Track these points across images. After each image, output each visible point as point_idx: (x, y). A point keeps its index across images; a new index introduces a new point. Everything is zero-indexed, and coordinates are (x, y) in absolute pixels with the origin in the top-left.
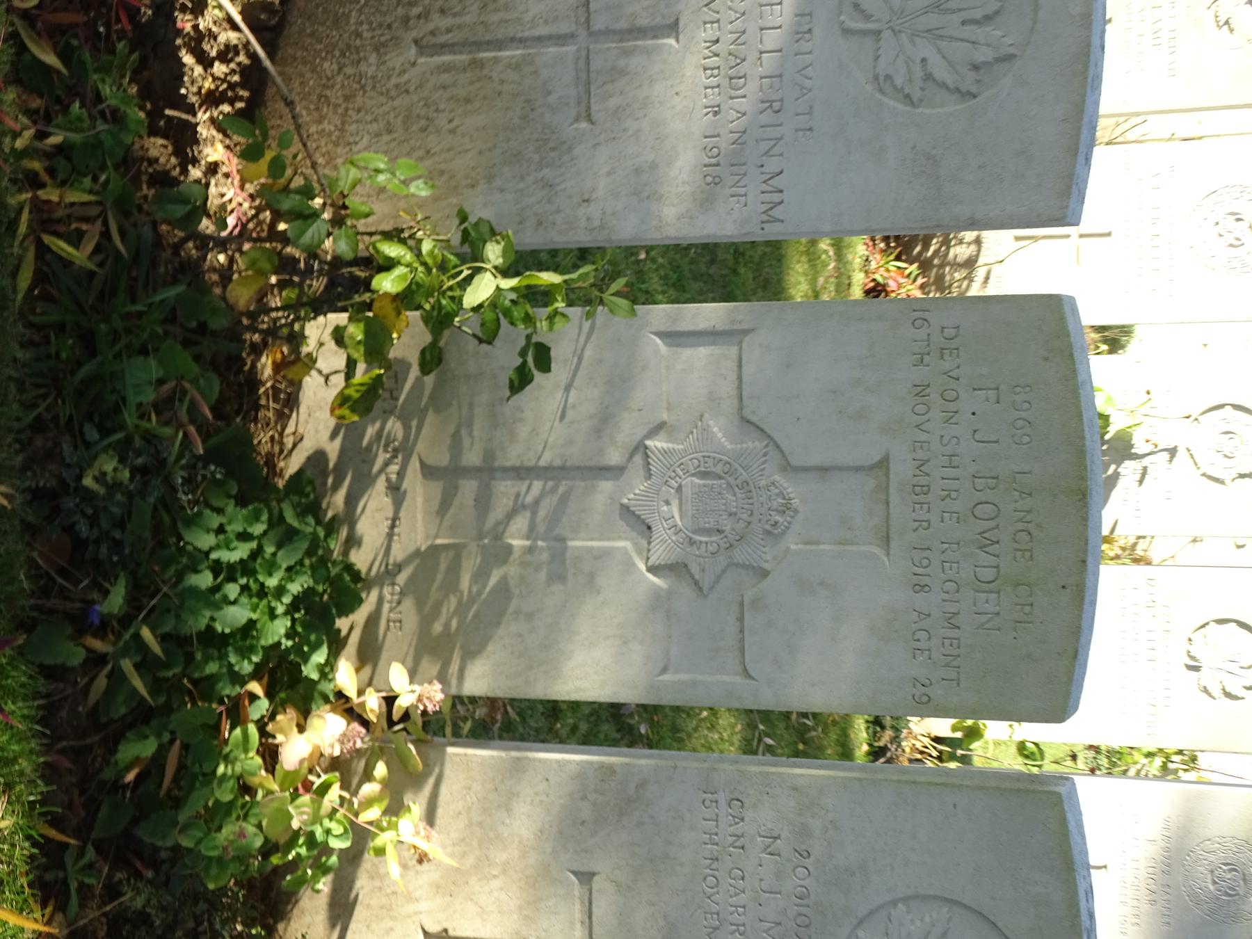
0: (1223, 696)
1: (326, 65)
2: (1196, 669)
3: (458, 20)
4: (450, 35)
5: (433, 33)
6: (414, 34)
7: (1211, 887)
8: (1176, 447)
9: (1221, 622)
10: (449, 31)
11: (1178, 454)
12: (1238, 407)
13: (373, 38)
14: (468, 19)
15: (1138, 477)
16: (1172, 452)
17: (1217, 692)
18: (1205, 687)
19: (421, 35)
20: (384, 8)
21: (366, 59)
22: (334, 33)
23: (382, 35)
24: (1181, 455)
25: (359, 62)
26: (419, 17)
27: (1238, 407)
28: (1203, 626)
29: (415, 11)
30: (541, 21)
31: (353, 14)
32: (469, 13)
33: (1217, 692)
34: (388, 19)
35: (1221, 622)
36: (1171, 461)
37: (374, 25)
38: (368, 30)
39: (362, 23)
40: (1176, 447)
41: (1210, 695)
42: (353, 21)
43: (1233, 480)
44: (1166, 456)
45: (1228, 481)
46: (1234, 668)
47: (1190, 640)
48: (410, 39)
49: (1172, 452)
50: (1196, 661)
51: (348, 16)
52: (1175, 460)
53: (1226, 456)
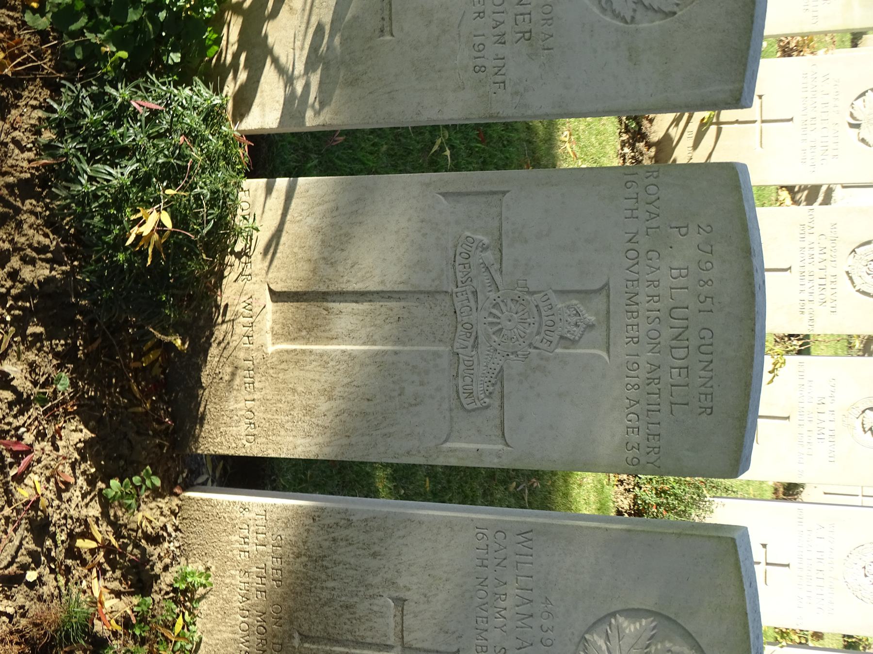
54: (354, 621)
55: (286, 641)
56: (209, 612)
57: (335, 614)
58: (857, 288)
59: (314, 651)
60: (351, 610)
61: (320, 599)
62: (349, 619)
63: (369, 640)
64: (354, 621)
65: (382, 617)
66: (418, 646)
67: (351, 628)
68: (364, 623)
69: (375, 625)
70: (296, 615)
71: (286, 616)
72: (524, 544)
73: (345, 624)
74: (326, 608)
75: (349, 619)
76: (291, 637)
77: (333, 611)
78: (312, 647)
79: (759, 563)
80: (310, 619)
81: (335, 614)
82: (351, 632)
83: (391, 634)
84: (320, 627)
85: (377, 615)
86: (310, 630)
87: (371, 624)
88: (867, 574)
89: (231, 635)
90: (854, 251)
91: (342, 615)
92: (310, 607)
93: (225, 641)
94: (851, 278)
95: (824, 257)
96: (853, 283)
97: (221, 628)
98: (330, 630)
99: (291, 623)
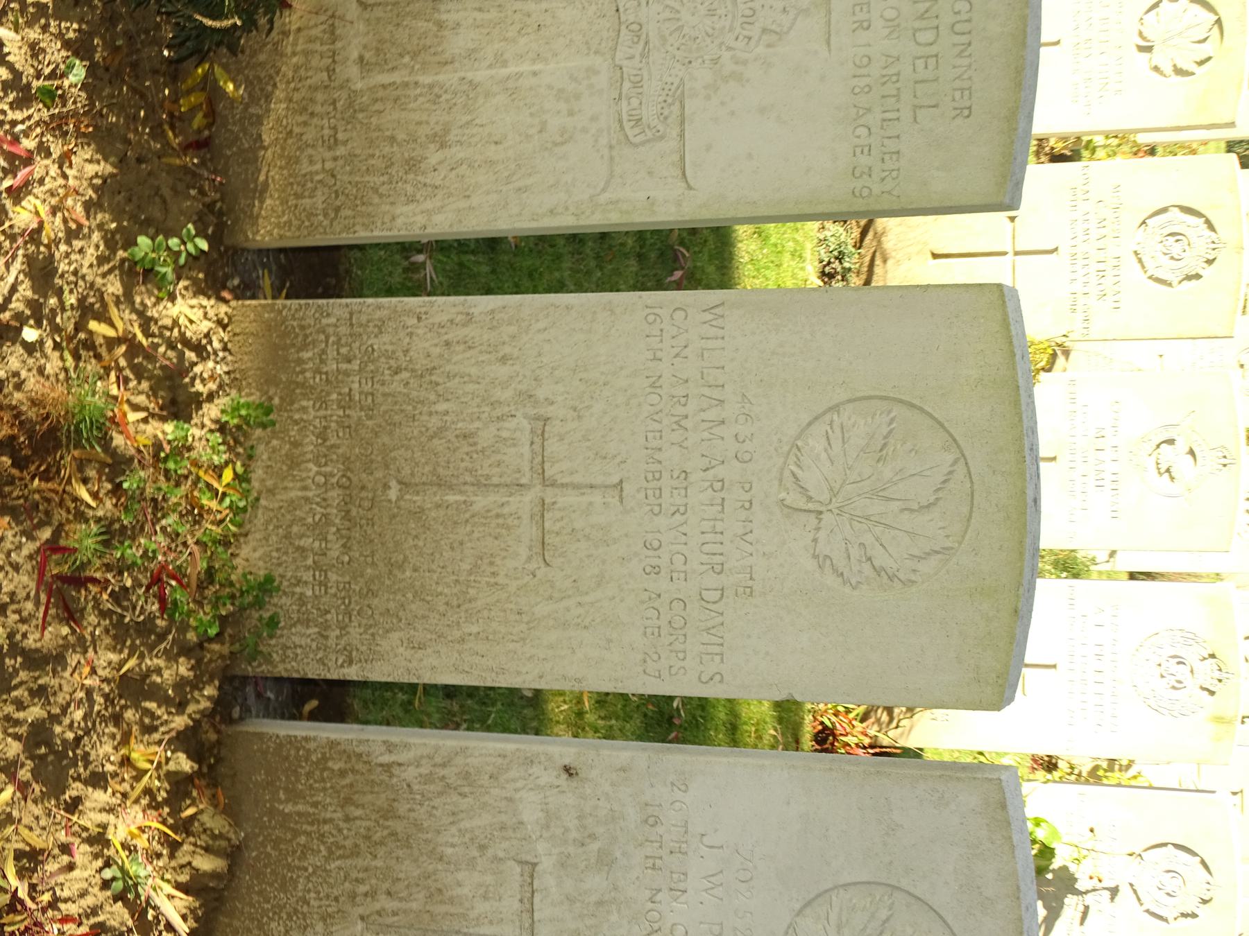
1: (273, 925)
3: (403, 905)
4: (396, 918)
5: (379, 913)
6: (360, 910)
10: (395, 914)
11: (1119, 894)
13: (320, 907)
14: (414, 905)
16: (1114, 892)
19: (368, 913)
20: (332, 881)
21: (312, 926)
22: (282, 895)
23: (330, 906)
24: (1125, 893)
25: (305, 928)
26: (366, 895)
29: (362, 889)
30: (486, 921)
31: (301, 880)
32: (415, 900)
34: (336, 892)
36: (1112, 899)
37: (322, 895)
38: (315, 899)
39: (309, 891)
42: (300, 887)
44: (1107, 894)
48: (356, 915)
49: (1114, 892)
51: (295, 882)
54: (475, 456)
55: (379, 493)
56: (269, 463)
57: (449, 448)
58: (1149, 274)
59: (418, 504)
60: (471, 440)
61: (427, 430)
62: (467, 454)
63: (495, 480)
64: (475, 456)
65: (514, 445)
66: (565, 481)
67: (470, 466)
68: (489, 457)
69: (505, 458)
70: (392, 454)
71: (379, 458)
72: (714, 323)
73: (462, 460)
74: (436, 441)
75: (467, 454)
76: (386, 487)
77: (446, 445)
78: (415, 498)
80: (412, 458)
81: (449, 448)
82: (471, 471)
83: (526, 468)
84: (427, 469)
85: (508, 443)
86: (412, 474)
87: (499, 457)
89: (300, 494)
90: (1144, 222)
91: (458, 448)
92: (413, 442)
93: (292, 501)
94: (1140, 261)
95: (1103, 232)
96: (1143, 267)
97: (286, 484)
98: (440, 470)
99: (387, 467)
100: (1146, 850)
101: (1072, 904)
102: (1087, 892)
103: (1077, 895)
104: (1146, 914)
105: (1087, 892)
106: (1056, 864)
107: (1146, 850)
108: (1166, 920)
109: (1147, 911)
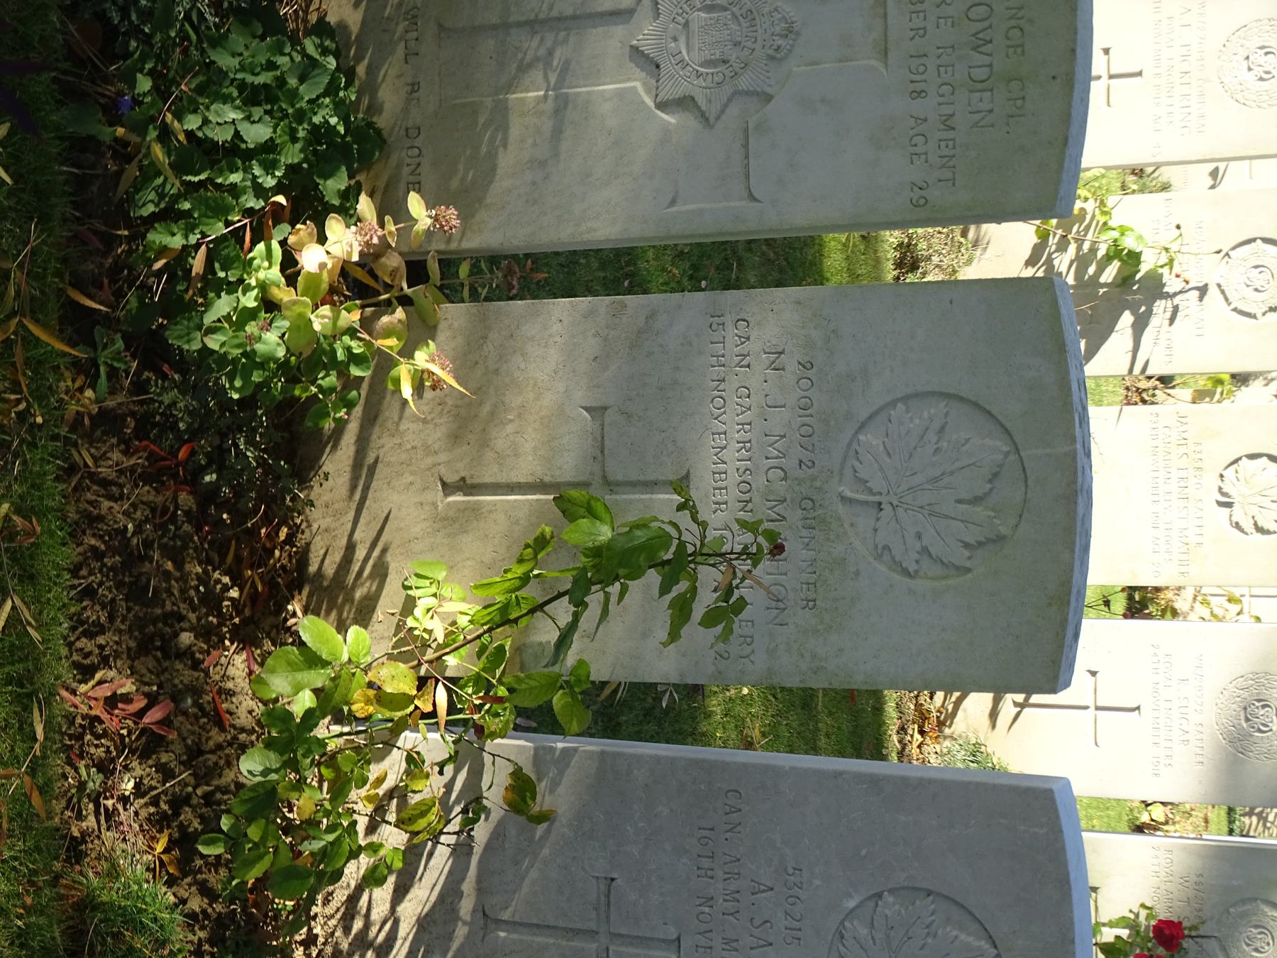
0: (1254, 531)
2: (1229, 505)
7: (1245, 725)
8: (1206, 285)
9: (1252, 457)
11: (1208, 293)
12: (1266, 240)
15: (1168, 315)
16: (1203, 291)
17: (1248, 525)
18: (1237, 523)
24: (1213, 292)
27: (1266, 240)
28: (1236, 461)
33: (1248, 525)
35: (1252, 457)
36: (1201, 299)
40: (1206, 285)
41: (1242, 531)
43: (1264, 314)
44: (1196, 293)
45: (1259, 315)
46: (1266, 502)
47: (1222, 476)
49: (1203, 291)
50: (1229, 497)
52: (1206, 298)
53: (1256, 290)
79: (1099, 78)
88: (1252, 66)
100: (1234, 248)
101: (1161, 308)
102: (1175, 294)
103: (1166, 299)
104: (1234, 313)
105: (1175, 294)
106: (1144, 268)
107: (1234, 248)
108: (1254, 317)
109: (1235, 310)
